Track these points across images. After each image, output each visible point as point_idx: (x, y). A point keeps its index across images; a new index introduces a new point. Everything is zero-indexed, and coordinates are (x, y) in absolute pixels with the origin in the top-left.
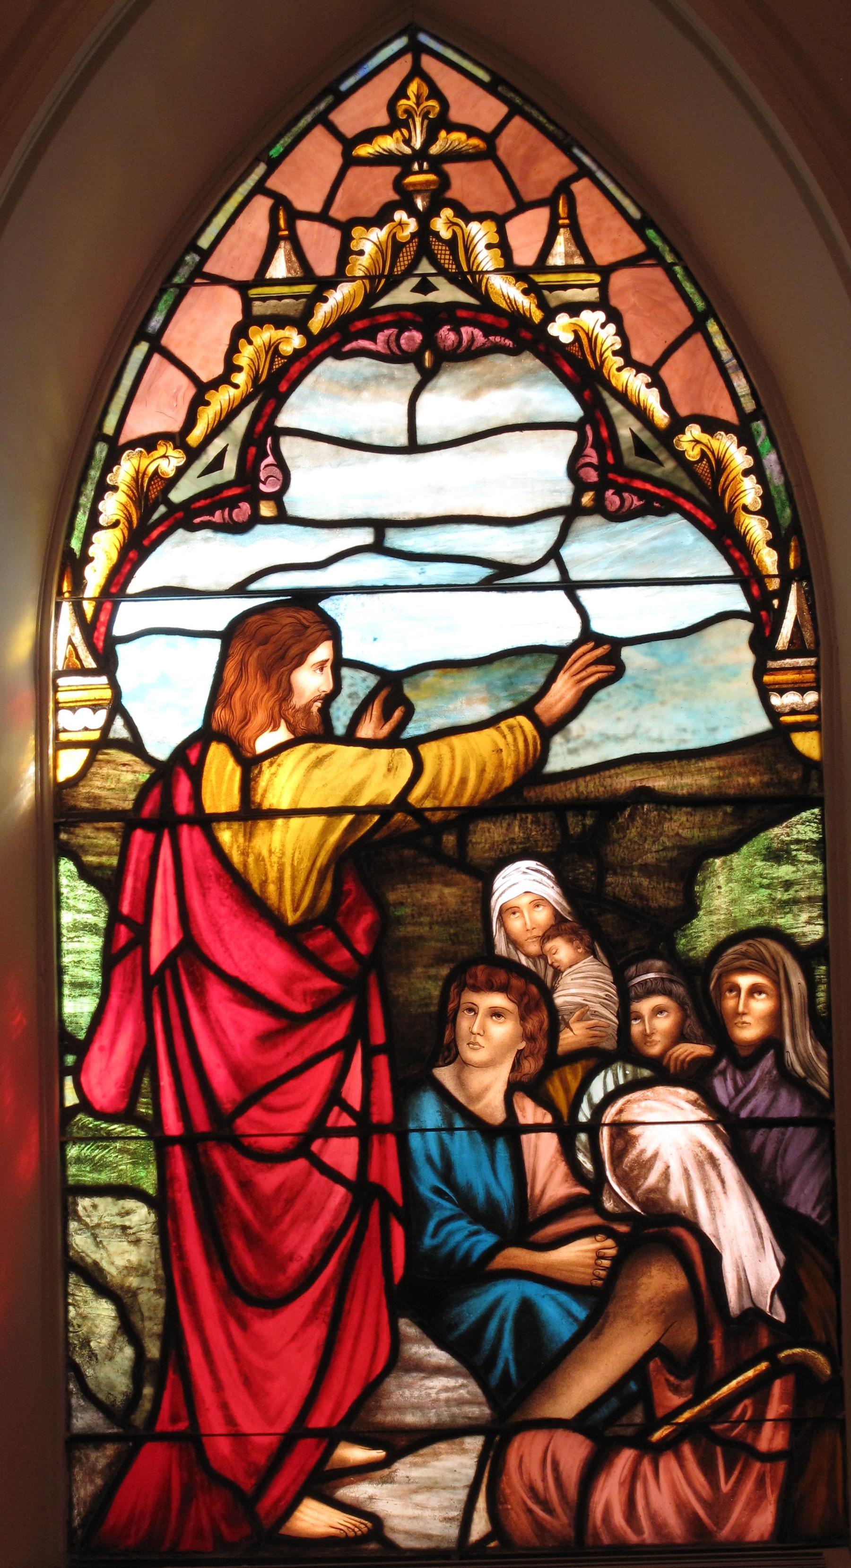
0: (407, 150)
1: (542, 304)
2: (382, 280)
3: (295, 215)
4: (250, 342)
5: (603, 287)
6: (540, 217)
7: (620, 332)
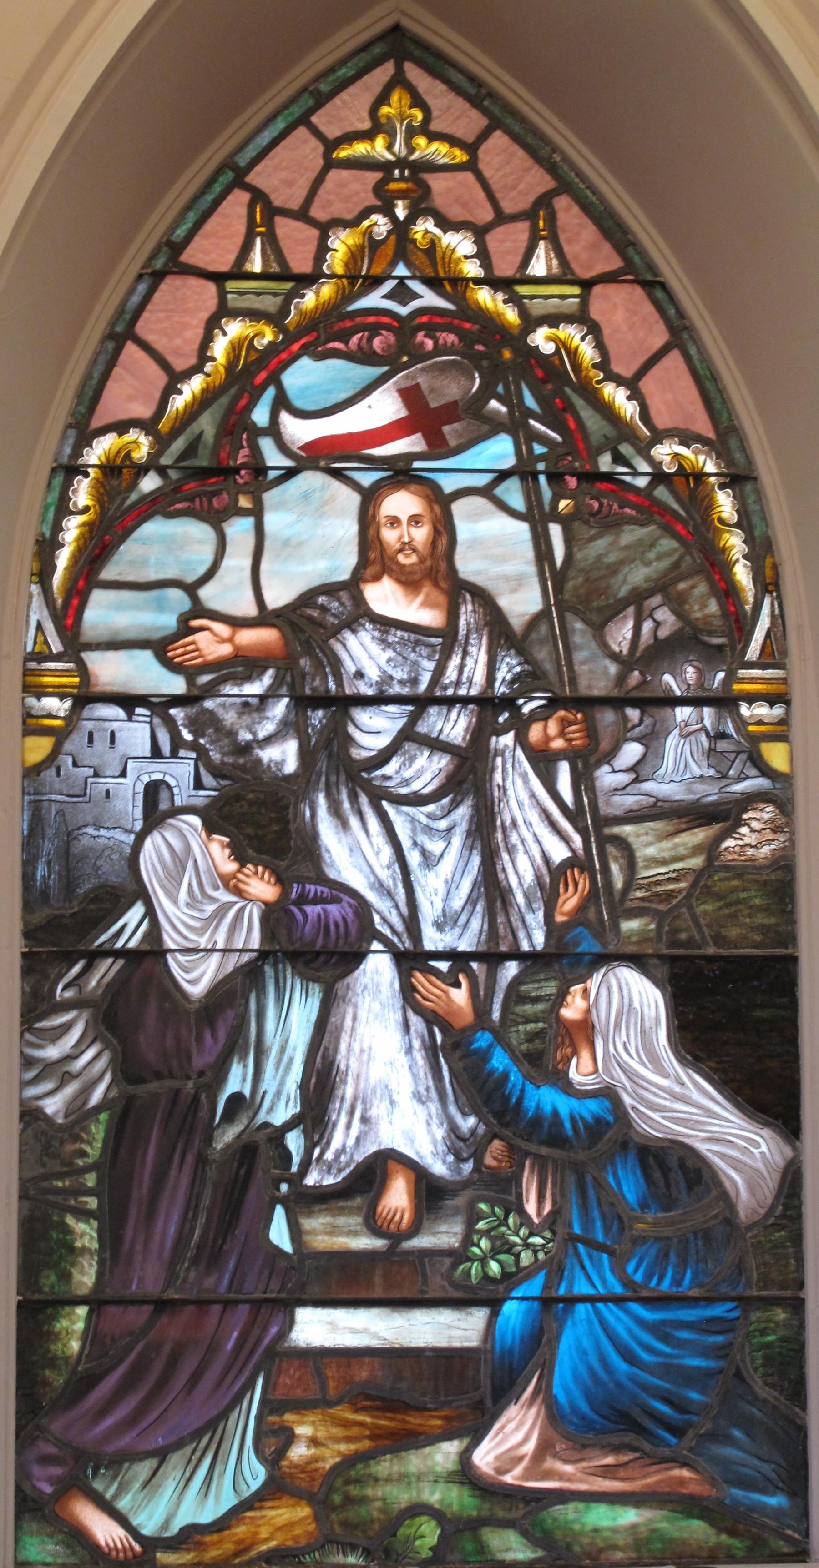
0: (390, 157)
1: (523, 313)
2: (359, 280)
3: (272, 212)
4: (225, 334)
5: (584, 299)
6: (520, 231)
7: (600, 346)
